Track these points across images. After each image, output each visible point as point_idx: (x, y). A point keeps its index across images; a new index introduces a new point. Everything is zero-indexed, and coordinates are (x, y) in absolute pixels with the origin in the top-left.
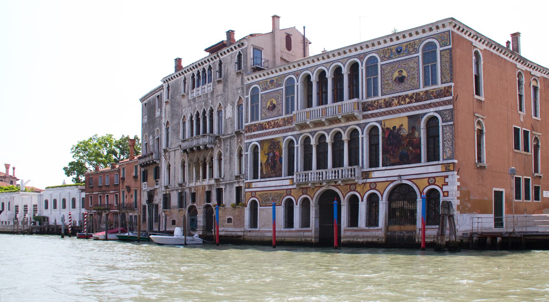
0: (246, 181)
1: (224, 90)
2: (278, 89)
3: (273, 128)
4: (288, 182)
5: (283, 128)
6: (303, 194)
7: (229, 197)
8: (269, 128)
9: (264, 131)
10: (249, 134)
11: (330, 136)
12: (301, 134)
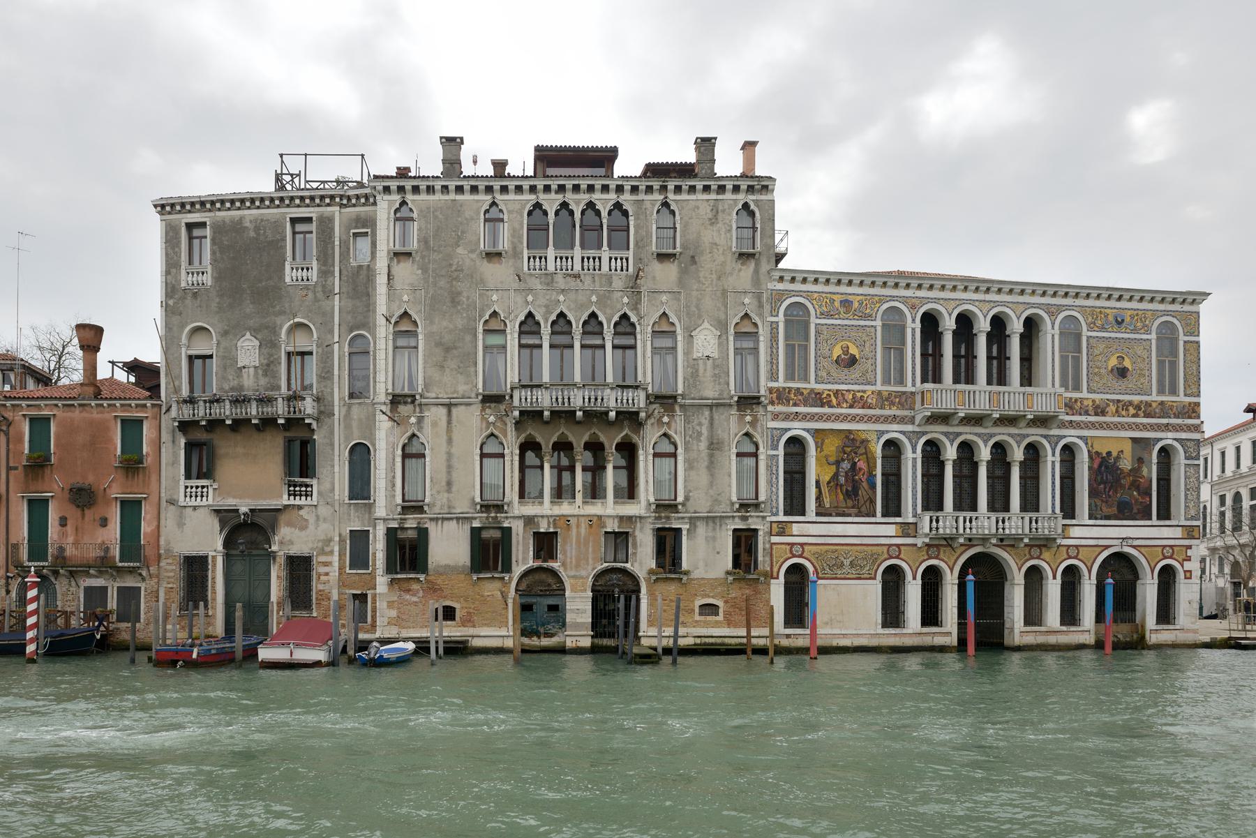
0: (774, 519)
1: (681, 282)
2: (862, 323)
3: (851, 407)
4: (891, 530)
5: (878, 412)
6: (930, 558)
7: (706, 555)
8: (839, 405)
9: (826, 410)
10: (779, 408)
11: (989, 449)
12: (924, 433)
